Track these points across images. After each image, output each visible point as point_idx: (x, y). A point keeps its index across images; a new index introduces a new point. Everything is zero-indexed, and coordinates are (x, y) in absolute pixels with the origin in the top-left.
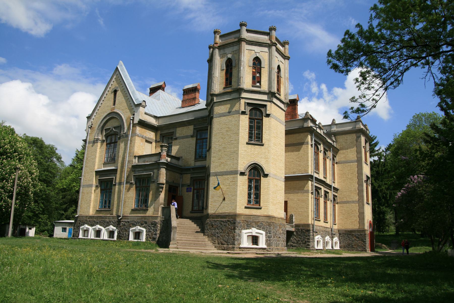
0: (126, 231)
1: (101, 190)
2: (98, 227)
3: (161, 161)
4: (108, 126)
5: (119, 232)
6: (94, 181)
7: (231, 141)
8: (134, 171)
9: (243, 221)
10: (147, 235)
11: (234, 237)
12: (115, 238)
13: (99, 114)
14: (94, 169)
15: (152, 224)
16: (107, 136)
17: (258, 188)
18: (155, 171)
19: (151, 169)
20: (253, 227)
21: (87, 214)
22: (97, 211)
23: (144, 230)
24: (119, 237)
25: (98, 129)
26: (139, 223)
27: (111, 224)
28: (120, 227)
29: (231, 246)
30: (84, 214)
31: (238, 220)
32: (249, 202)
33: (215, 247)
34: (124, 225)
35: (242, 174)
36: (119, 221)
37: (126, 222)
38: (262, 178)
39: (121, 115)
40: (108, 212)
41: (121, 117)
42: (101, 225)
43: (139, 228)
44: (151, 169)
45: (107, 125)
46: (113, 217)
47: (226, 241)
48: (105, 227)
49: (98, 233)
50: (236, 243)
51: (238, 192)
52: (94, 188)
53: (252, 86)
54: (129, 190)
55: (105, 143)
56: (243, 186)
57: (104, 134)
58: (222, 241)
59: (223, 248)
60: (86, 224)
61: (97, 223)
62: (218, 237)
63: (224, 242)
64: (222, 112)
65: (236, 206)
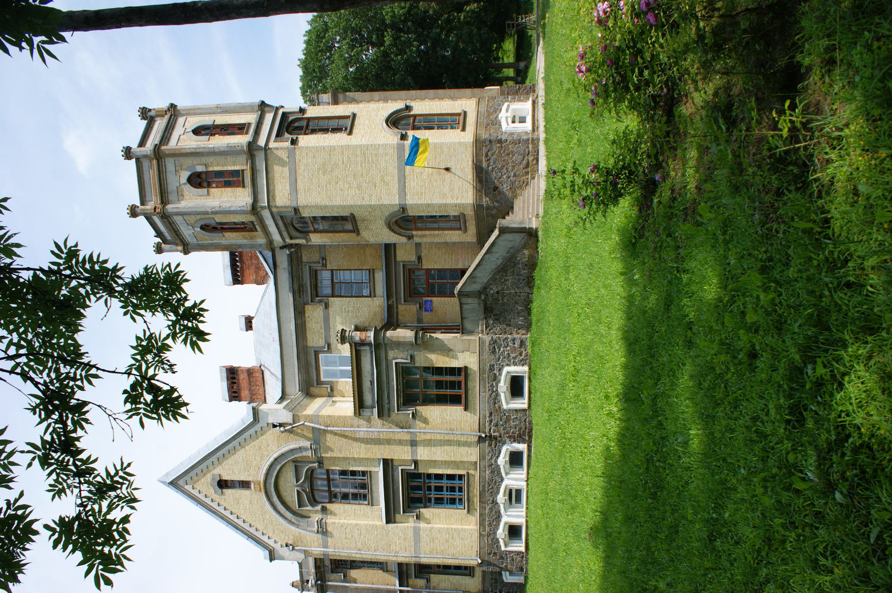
0: (508, 419)
1: (425, 507)
2: (501, 498)
3: (372, 339)
4: (292, 498)
5: (510, 437)
6: (406, 525)
8: (389, 410)
10: (515, 364)
11: (514, 143)
12: (522, 447)
13: (266, 527)
14: (383, 528)
15: (494, 352)
16: (314, 502)
18: (391, 354)
19: (387, 366)
20: (497, 117)
21: (476, 535)
22: (468, 512)
23: (506, 369)
24: (519, 439)
25: (298, 526)
26: (492, 386)
27: (496, 461)
28: (500, 436)
29: (530, 146)
30: (476, 548)
31: (484, 135)
33: (534, 178)
34: (496, 425)
36: (490, 437)
37: (491, 421)
38: (412, 113)
39: (272, 459)
40: (471, 479)
41: (276, 459)
42: (498, 492)
43: (502, 384)
44: (387, 366)
45: (290, 505)
46: (482, 457)
47: (521, 157)
48: (502, 480)
49: (515, 496)
50: (525, 137)
52: (422, 525)
53: (247, 133)
54: (425, 421)
55: (329, 506)
57: (310, 508)
58: (521, 166)
59: (535, 162)
60: (495, 533)
61: (495, 503)
62: (515, 175)
63: (524, 162)
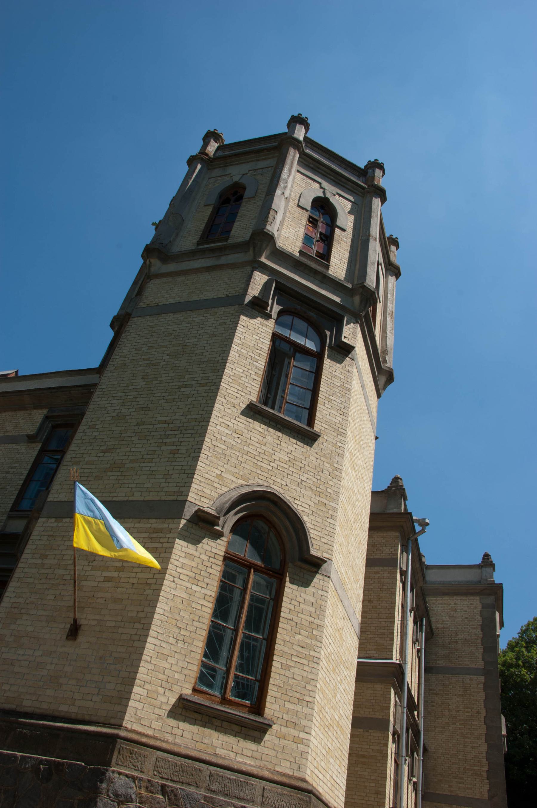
7: (180, 387)
9: (149, 786)
17: (266, 617)
32: (206, 676)
35: (204, 525)
51: (162, 607)
56: (195, 580)
64: (171, 301)
65: (130, 681)
